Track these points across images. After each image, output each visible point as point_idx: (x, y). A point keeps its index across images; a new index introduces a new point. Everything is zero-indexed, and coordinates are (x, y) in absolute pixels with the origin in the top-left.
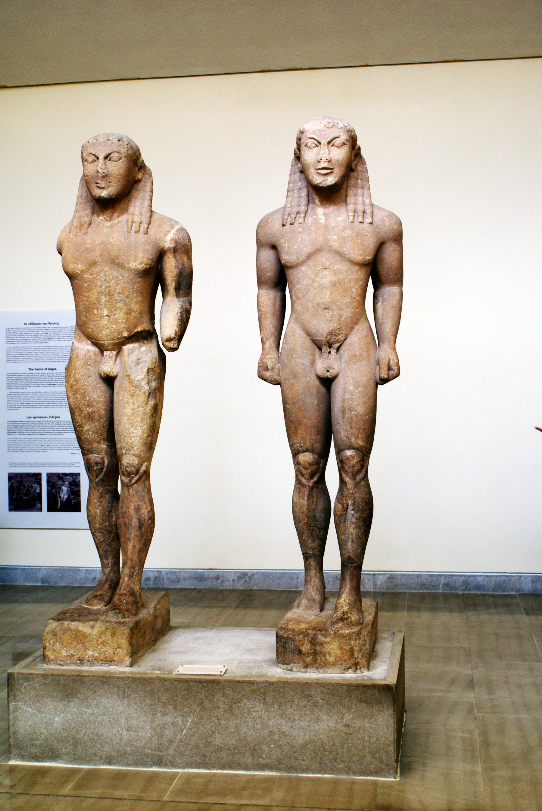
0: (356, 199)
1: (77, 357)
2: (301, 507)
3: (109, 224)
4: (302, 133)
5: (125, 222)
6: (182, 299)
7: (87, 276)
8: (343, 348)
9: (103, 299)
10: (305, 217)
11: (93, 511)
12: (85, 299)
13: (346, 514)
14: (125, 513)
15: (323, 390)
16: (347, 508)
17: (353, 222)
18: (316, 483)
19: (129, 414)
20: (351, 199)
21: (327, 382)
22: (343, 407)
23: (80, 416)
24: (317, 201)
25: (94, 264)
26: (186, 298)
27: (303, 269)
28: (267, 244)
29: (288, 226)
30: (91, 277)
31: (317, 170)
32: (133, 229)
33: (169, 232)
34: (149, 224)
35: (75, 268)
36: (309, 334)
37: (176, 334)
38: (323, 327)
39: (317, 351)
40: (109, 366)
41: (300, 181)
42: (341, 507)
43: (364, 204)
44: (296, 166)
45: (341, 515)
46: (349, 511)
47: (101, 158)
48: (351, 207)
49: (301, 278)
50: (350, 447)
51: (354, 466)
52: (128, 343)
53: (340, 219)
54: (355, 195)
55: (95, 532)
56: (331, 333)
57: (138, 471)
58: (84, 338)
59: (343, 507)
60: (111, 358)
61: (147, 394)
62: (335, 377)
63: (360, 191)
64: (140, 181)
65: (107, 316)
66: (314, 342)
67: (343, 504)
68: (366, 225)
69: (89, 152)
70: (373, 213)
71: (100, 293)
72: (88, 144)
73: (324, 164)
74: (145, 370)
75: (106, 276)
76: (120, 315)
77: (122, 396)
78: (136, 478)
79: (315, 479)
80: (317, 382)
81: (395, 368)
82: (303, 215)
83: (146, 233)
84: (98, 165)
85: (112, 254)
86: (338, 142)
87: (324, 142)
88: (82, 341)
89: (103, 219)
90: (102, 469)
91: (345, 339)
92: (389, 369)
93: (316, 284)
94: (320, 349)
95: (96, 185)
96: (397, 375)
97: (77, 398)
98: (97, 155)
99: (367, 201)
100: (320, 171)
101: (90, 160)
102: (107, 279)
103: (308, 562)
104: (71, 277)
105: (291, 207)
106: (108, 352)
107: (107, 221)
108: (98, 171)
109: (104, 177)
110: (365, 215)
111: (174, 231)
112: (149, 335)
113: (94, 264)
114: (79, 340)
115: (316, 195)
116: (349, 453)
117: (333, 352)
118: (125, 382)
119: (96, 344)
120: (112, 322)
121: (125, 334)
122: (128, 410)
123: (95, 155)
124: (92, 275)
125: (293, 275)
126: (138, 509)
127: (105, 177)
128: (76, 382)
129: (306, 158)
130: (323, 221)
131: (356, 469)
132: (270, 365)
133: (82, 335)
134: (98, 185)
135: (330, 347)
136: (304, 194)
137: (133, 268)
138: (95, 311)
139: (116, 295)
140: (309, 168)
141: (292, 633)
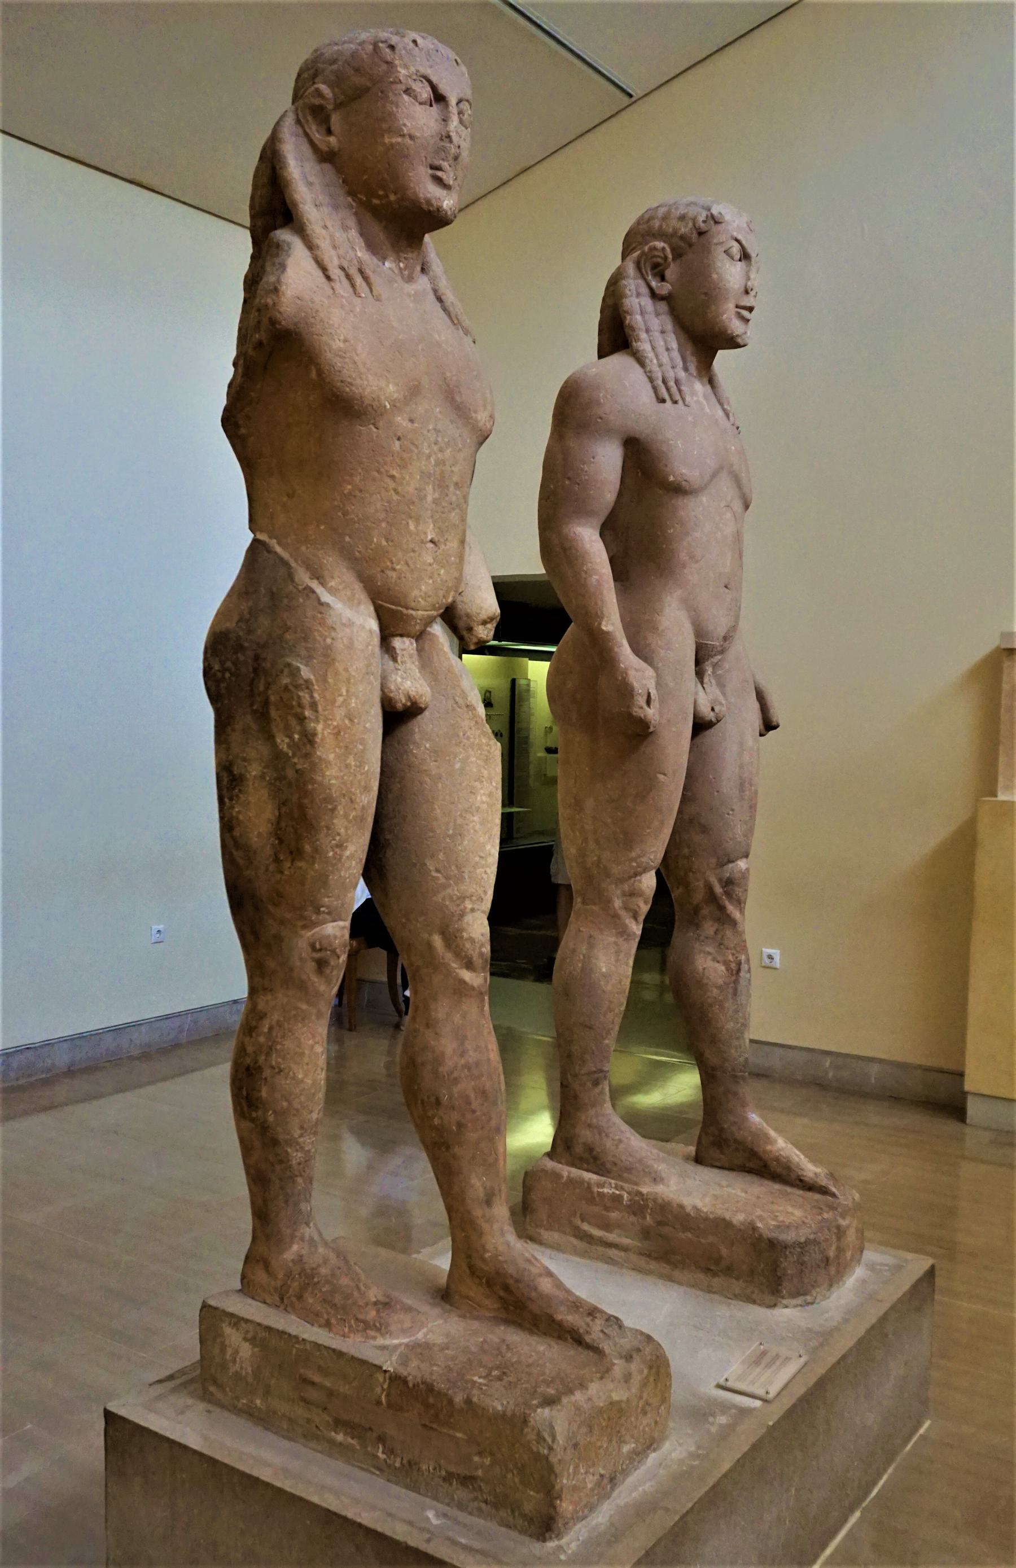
1: (350, 647)
2: (620, 982)
3: (410, 288)
4: (716, 222)
5: (431, 297)
9: (431, 494)
12: (392, 484)
13: (736, 982)
14: (477, 1064)
16: (739, 970)
22: (740, 777)
23: (346, 816)
24: (692, 368)
27: (704, 499)
30: (409, 425)
31: (737, 307)
35: (381, 389)
36: (700, 632)
42: (723, 968)
44: (641, 282)
45: (727, 984)
47: (453, 101)
58: (362, 596)
59: (728, 969)
60: (411, 656)
62: (718, 721)
65: (432, 541)
67: (726, 963)
69: (423, 70)
71: (425, 476)
72: (412, 45)
75: (437, 431)
84: (445, 120)
85: (448, 374)
88: (359, 603)
89: (396, 271)
94: (698, 662)
95: (430, 172)
97: (348, 766)
98: (444, 88)
100: (745, 313)
102: (440, 439)
103: (597, 1090)
105: (660, 365)
107: (402, 277)
108: (449, 137)
114: (350, 601)
115: (693, 354)
123: (434, 88)
124: (412, 421)
128: (351, 720)
133: (358, 587)
134: (439, 174)
136: (674, 345)
138: (412, 527)
139: (452, 488)
140: (727, 299)
141: (810, 1230)
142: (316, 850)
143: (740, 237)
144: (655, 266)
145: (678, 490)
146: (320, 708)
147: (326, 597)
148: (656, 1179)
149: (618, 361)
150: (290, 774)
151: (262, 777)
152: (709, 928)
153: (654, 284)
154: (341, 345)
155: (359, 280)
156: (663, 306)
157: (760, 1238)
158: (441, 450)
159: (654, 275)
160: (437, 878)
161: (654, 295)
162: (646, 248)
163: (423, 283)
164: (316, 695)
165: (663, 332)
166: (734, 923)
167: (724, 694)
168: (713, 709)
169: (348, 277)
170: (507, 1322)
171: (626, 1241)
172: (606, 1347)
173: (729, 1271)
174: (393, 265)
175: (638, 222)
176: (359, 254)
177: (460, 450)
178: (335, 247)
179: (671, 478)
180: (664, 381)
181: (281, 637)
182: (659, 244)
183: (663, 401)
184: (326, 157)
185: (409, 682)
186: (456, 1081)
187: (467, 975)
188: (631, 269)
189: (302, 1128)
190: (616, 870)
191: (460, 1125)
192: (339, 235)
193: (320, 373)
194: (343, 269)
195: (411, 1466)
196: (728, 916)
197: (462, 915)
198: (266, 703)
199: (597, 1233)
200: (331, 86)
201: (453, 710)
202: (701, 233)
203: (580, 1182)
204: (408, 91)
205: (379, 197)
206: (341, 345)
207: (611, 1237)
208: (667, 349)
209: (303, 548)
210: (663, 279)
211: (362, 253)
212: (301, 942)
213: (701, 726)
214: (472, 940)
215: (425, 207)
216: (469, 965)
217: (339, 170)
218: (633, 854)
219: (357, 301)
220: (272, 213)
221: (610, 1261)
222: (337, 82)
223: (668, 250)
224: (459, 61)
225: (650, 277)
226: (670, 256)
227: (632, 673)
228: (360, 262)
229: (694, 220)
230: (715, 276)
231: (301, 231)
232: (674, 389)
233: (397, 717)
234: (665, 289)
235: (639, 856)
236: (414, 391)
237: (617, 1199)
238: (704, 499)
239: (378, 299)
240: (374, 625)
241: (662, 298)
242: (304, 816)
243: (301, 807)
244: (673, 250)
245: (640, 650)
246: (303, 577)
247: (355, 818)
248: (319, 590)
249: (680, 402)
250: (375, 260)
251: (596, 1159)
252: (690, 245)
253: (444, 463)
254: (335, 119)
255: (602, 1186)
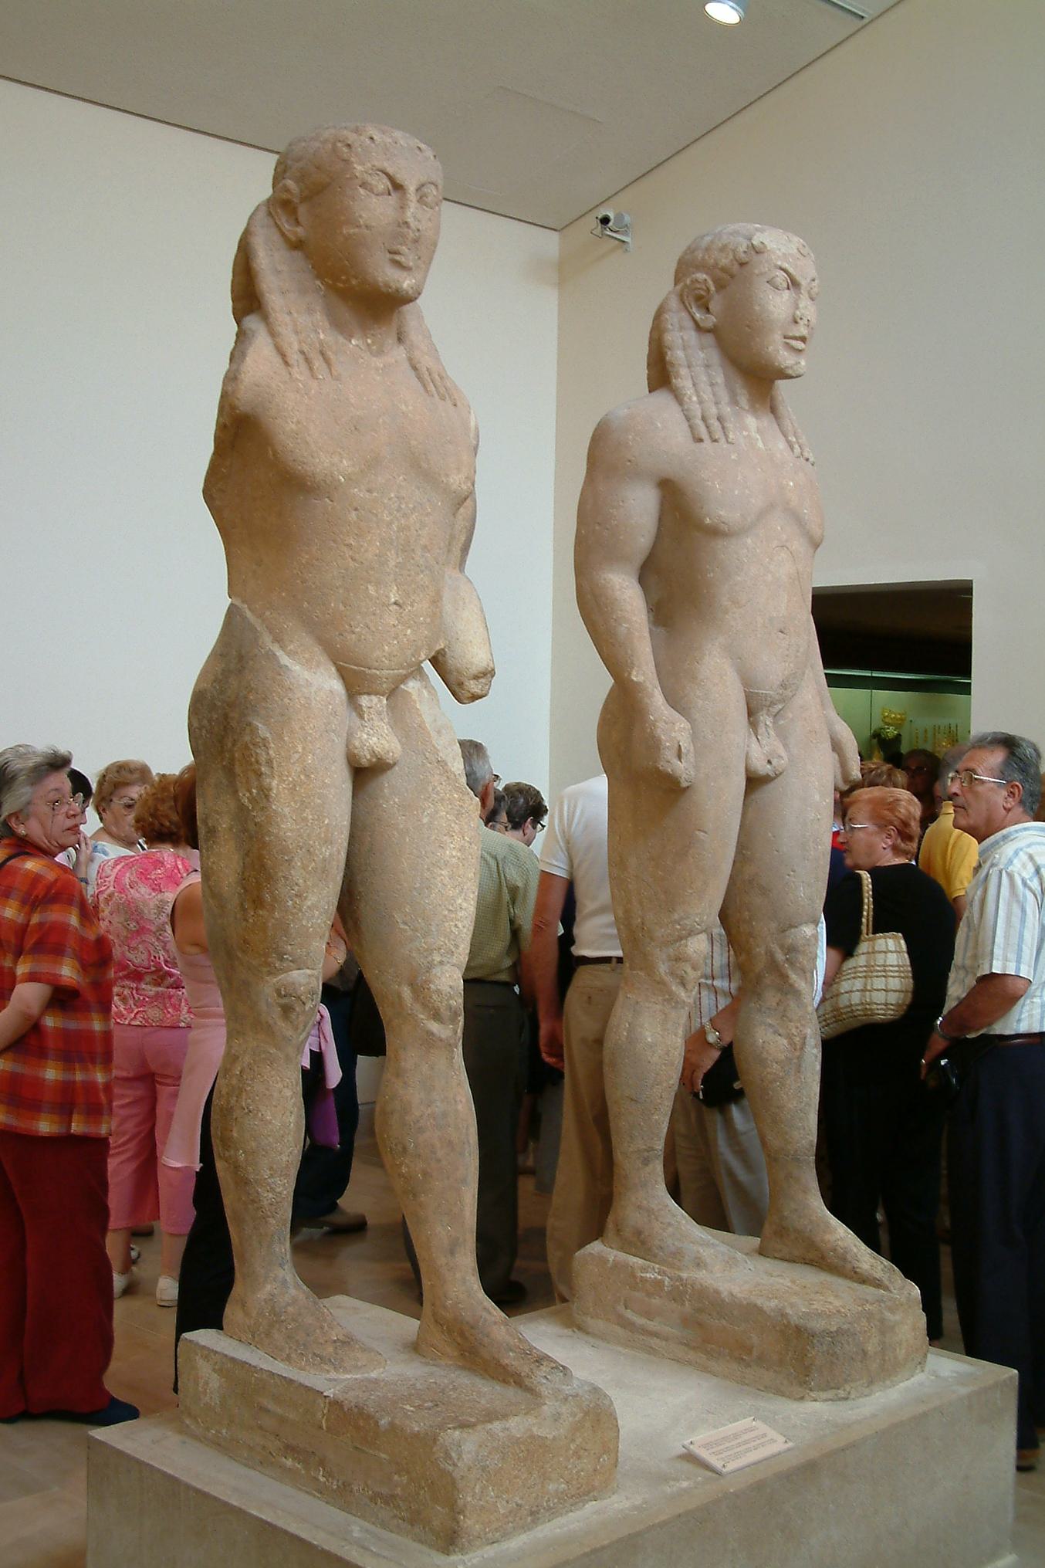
3: (378, 362)
5: (406, 365)
7: (358, 492)
11: (277, 1123)
12: (348, 553)
13: (799, 1058)
14: (445, 1115)
19: (454, 860)
24: (744, 400)
27: (749, 541)
30: (367, 495)
41: (702, 348)
42: (785, 1042)
44: (684, 314)
46: (808, 1049)
55: (272, 1176)
58: (323, 658)
59: (792, 1043)
60: (379, 713)
62: (777, 776)
65: (395, 603)
67: (790, 1037)
73: (803, 331)
77: (431, 816)
84: (403, 207)
85: (414, 443)
93: (769, 578)
94: (751, 713)
95: (388, 256)
97: (305, 820)
98: (400, 177)
100: (794, 343)
101: (381, 187)
103: (648, 1169)
105: (701, 402)
106: (375, 699)
109: (416, 241)
114: (308, 663)
118: (437, 777)
122: (451, 853)
124: (369, 491)
128: (308, 776)
129: (771, 308)
130: (760, 444)
133: (317, 649)
134: (397, 258)
136: (720, 379)
137: (454, 487)
138: (372, 590)
139: (419, 552)
142: (275, 899)
143: (786, 266)
144: (699, 298)
145: (715, 532)
146: (275, 765)
147: (285, 660)
148: (699, 1263)
149: (662, 397)
150: (251, 827)
151: (231, 829)
152: (771, 998)
153: (698, 316)
154: (293, 426)
155: (318, 363)
156: (709, 339)
157: (788, 1326)
158: (405, 515)
159: (699, 307)
160: (405, 931)
161: (698, 328)
162: (688, 282)
163: (399, 354)
164: (271, 752)
165: (707, 366)
166: (797, 994)
167: (785, 746)
168: (769, 762)
169: (307, 360)
170: (463, 1368)
171: (667, 1330)
172: (544, 1391)
173: (761, 1360)
174: (360, 343)
175: (685, 253)
176: (322, 336)
177: (428, 514)
178: (297, 333)
179: (708, 521)
180: (704, 419)
181: (246, 697)
182: (701, 276)
183: (701, 440)
184: (297, 245)
185: (378, 738)
186: (421, 1130)
187: (434, 1027)
188: (674, 303)
189: (271, 1169)
190: (659, 933)
191: (425, 1174)
192: (303, 320)
193: (275, 453)
194: (302, 352)
195: (346, 1486)
196: (791, 985)
197: (430, 967)
198: (232, 760)
199: (640, 1321)
200: (297, 181)
201: (424, 765)
202: (742, 264)
203: (626, 1266)
204: (364, 185)
205: (344, 282)
206: (293, 426)
207: (652, 1325)
208: (712, 385)
209: (268, 613)
210: (708, 310)
211: (325, 335)
212: (267, 989)
213: (754, 782)
214: (439, 992)
215: (384, 290)
216: (436, 1016)
217: (308, 257)
218: (676, 916)
219: (314, 384)
220: (247, 298)
221: (651, 1351)
222: (301, 179)
223: (710, 283)
224: (423, 146)
225: (694, 310)
226: (713, 288)
227: (661, 725)
228: (321, 343)
229: (734, 251)
230: (757, 308)
231: (265, 318)
232: (715, 425)
233: (364, 774)
234: (710, 321)
235: (682, 919)
236: (373, 463)
237: (659, 1284)
238: (749, 541)
239: (338, 379)
240: (337, 686)
241: (709, 331)
242: (263, 866)
243: (260, 858)
244: (716, 281)
245: (675, 701)
246: (267, 639)
247: (315, 870)
248: (279, 653)
249: (723, 440)
250: (341, 339)
251: (643, 1243)
252: (732, 276)
253: (407, 528)
254: (302, 211)
255: (644, 1270)
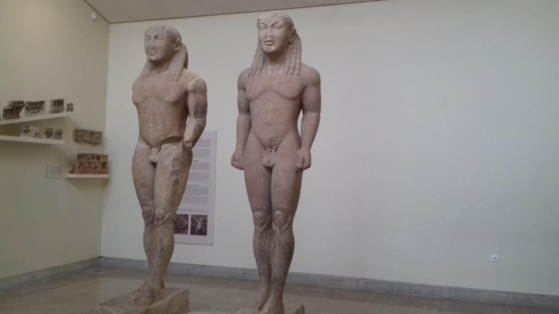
0: (290, 60)
3: (158, 76)
6: (198, 119)
7: (143, 105)
8: (279, 149)
9: (151, 118)
10: (260, 71)
15: (267, 173)
17: (287, 74)
18: (265, 229)
20: (287, 60)
21: (270, 169)
24: (268, 62)
25: (146, 98)
26: (201, 119)
27: (257, 101)
28: (242, 88)
29: (251, 77)
32: (170, 79)
33: (191, 80)
34: (180, 75)
36: (259, 140)
37: (191, 139)
38: (267, 135)
39: (264, 150)
40: (154, 157)
43: (295, 63)
48: (287, 65)
49: (255, 107)
50: (279, 209)
51: (280, 221)
52: (165, 143)
53: (280, 72)
54: (291, 58)
56: (271, 140)
57: (163, 218)
61: (171, 173)
63: (294, 56)
64: (178, 52)
66: (262, 145)
68: (295, 76)
70: (300, 68)
74: (172, 159)
76: (160, 127)
78: (162, 222)
79: (264, 227)
80: (264, 169)
81: (307, 162)
82: (259, 70)
83: (177, 81)
86: (277, 25)
87: (269, 25)
90: (150, 216)
91: (279, 144)
92: (303, 162)
94: (266, 149)
96: (309, 166)
99: (298, 61)
104: (137, 104)
110: (295, 70)
111: (194, 80)
112: (178, 139)
113: (146, 98)
116: (278, 212)
117: (273, 151)
119: (148, 143)
120: (156, 131)
121: (162, 138)
125: (253, 105)
126: (161, 240)
127: (154, 48)
130: (270, 73)
131: (281, 222)
132: (237, 158)
135: (271, 148)
136: (262, 57)
143: (263, 22)
240: (145, 146)
